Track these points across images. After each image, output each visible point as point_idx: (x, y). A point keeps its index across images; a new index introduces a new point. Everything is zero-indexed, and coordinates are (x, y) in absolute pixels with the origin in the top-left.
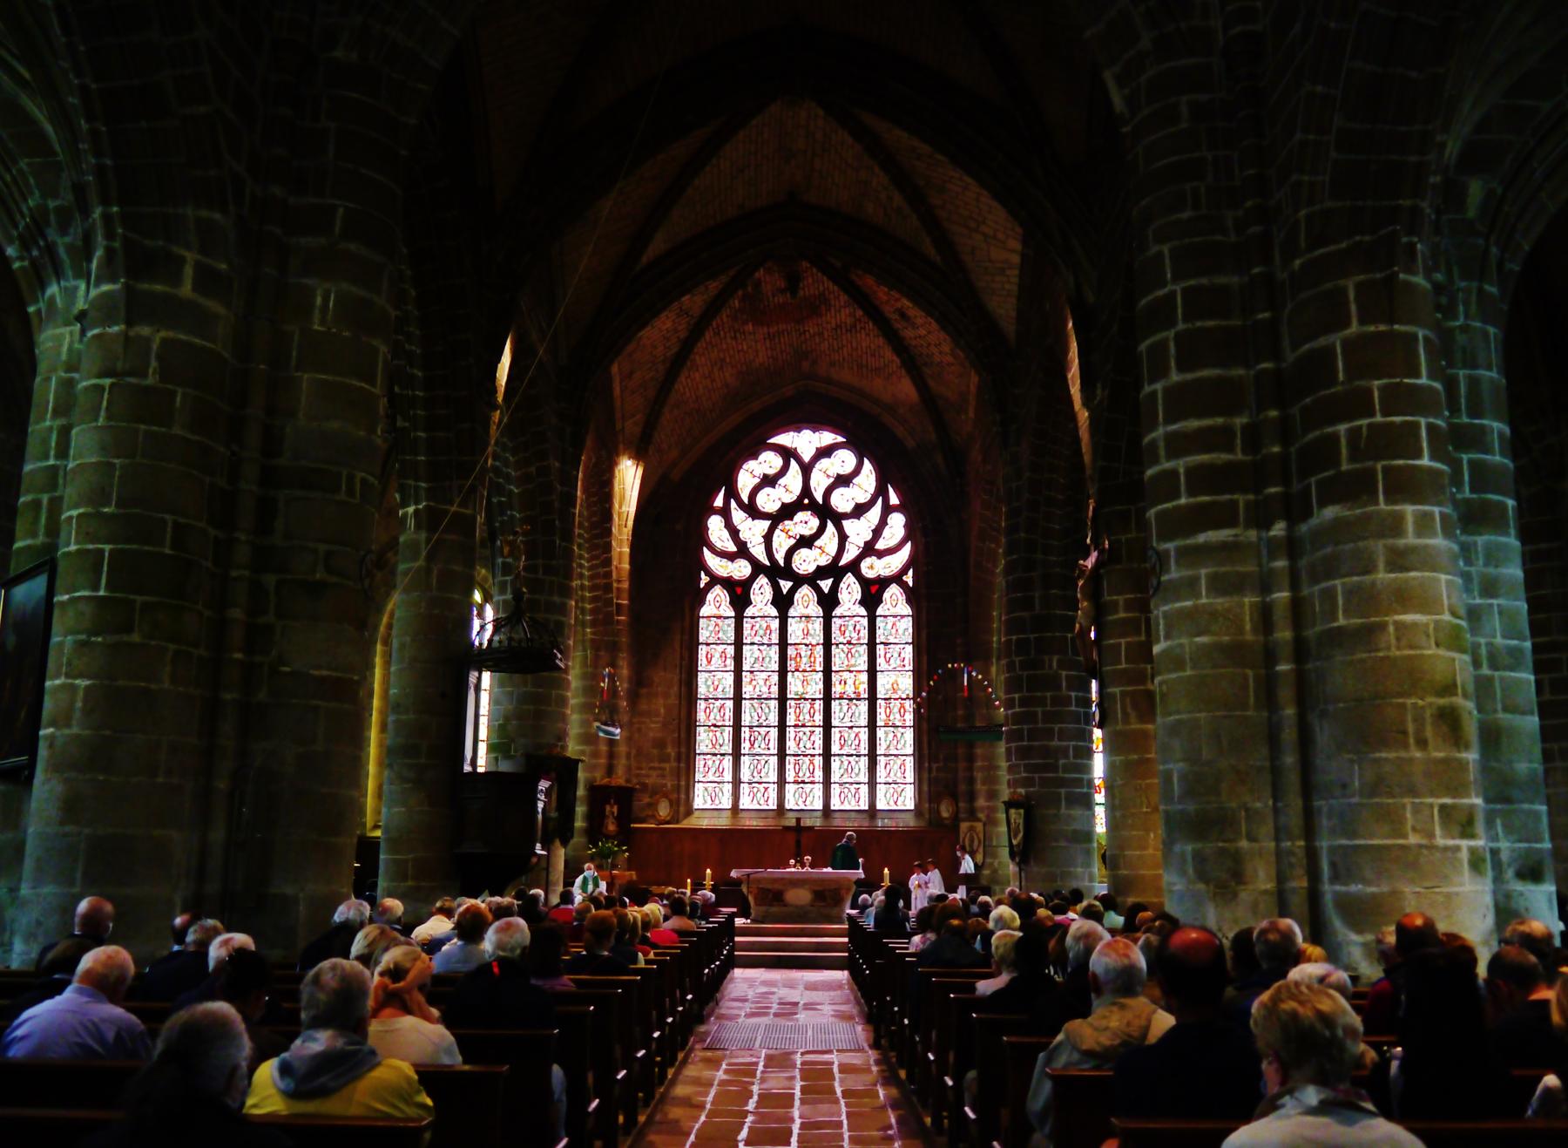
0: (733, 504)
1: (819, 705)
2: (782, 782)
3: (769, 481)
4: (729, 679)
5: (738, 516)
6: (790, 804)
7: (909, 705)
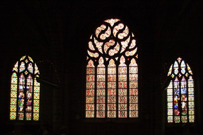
0: (95, 38)
1: (115, 90)
2: (106, 111)
3: (103, 32)
4: (94, 83)
5: (96, 41)
6: (108, 116)
7: (137, 90)
